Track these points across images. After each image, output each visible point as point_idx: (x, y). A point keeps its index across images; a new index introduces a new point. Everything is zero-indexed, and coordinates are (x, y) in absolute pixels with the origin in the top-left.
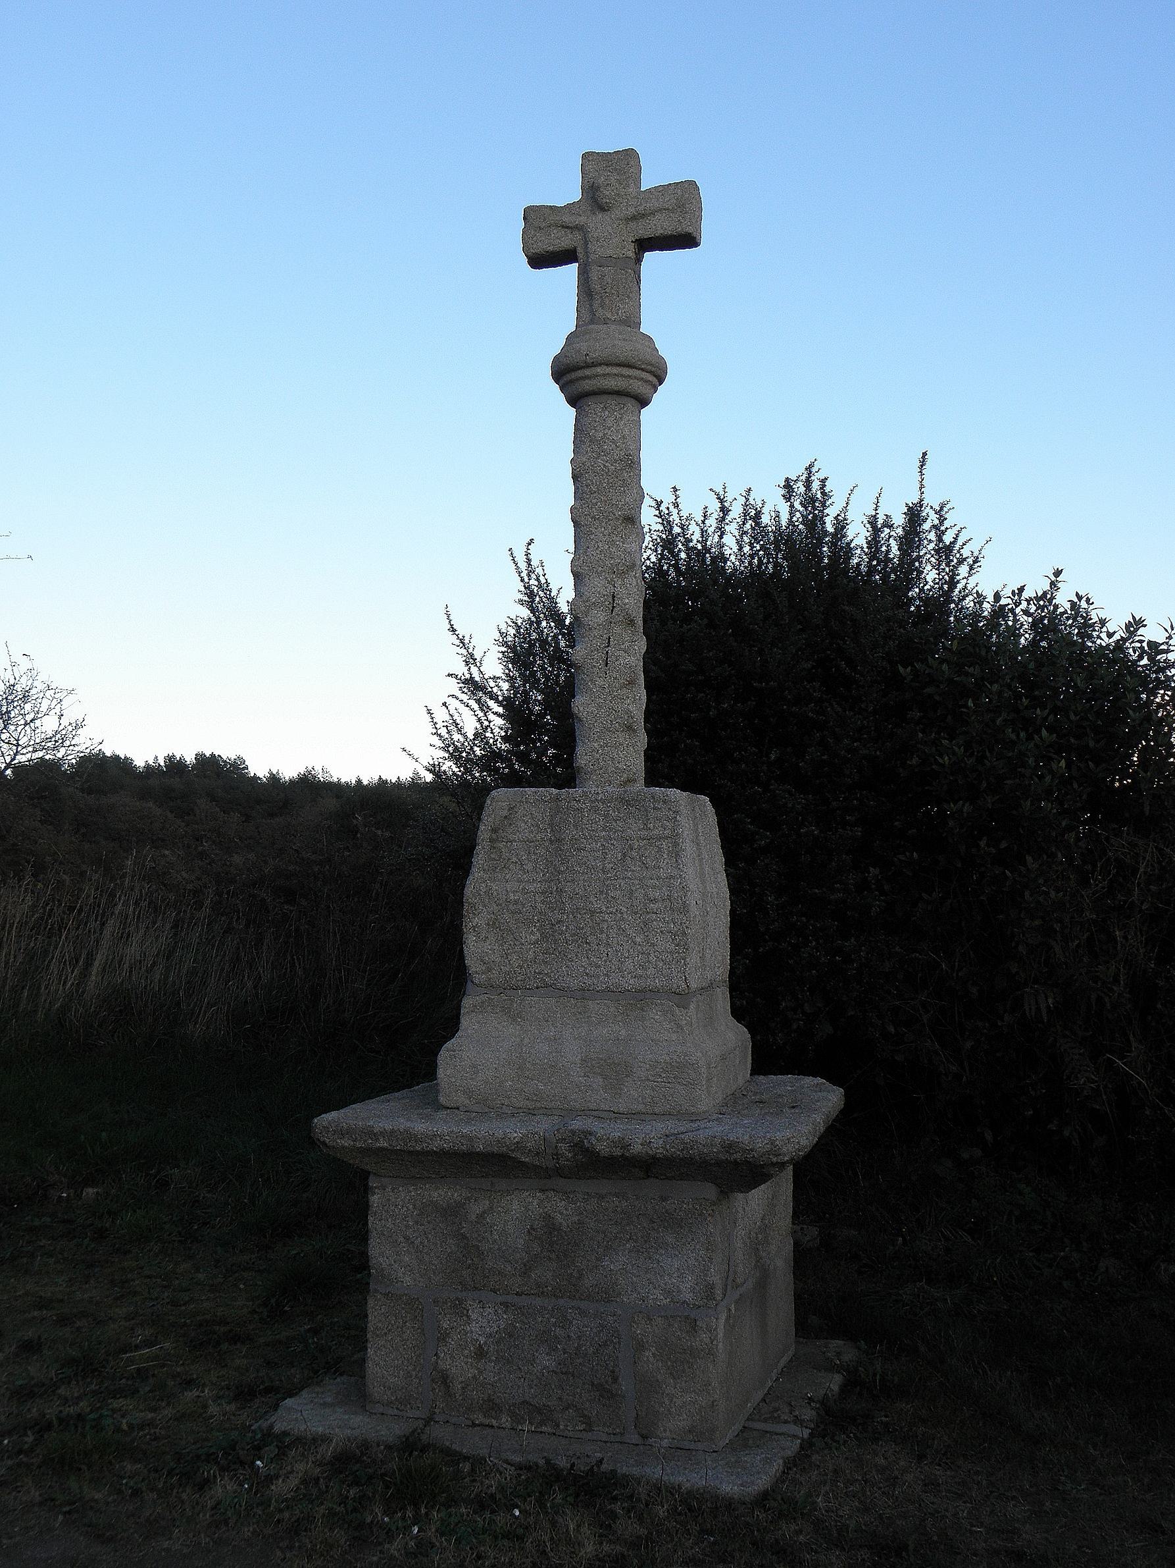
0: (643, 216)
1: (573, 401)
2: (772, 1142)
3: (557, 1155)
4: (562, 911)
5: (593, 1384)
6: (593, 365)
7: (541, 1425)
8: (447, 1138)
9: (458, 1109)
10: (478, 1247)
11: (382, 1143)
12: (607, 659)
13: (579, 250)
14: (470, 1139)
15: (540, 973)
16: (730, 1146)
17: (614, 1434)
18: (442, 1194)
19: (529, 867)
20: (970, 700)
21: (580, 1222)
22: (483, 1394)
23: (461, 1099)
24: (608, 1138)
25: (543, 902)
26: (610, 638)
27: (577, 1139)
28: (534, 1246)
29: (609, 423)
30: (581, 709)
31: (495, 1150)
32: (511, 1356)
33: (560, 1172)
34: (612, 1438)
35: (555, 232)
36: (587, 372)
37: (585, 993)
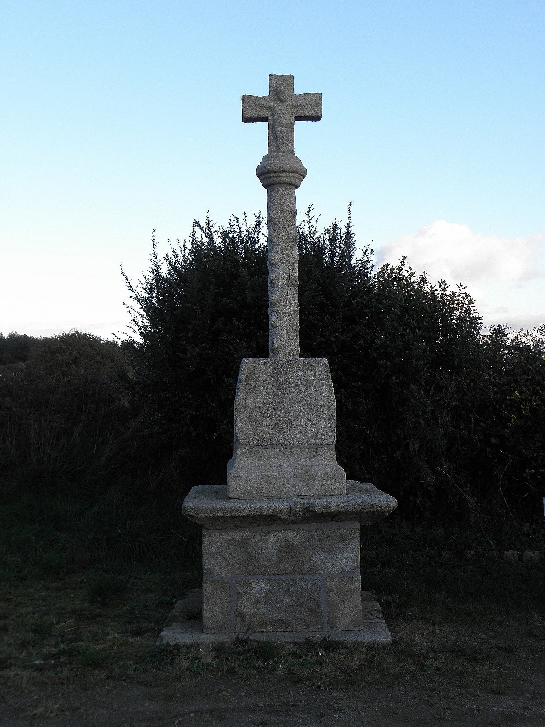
0: (300, 106)
1: (265, 186)
2: (387, 503)
3: (295, 514)
4: (280, 411)
5: (309, 609)
6: (282, 171)
7: (286, 629)
8: (250, 509)
9: (238, 499)
10: (255, 557)
11: (221, 514)
12: (287, 301)
13: (269, 118)
14: (261, 510)
15: (271, 438)
16: (372, 505)
17: (318, 628)
18: (238, 535)
19: (264, 392)
20: (455, 323)
21: (302, 542)
22: (259, 619)
23: (239, 494)
24: (321, 505)
25: (271, 407)
26: (288, 292)
27: (305, 507)
28: (281, 554)
29: (287, 197)
30: (276, 323)
31: (272, 513)
32: (272, 601)
33: (294, 522)
34: (318, 630)
35: (258, 108)
36: (279, 174)
37: (291, 446)
